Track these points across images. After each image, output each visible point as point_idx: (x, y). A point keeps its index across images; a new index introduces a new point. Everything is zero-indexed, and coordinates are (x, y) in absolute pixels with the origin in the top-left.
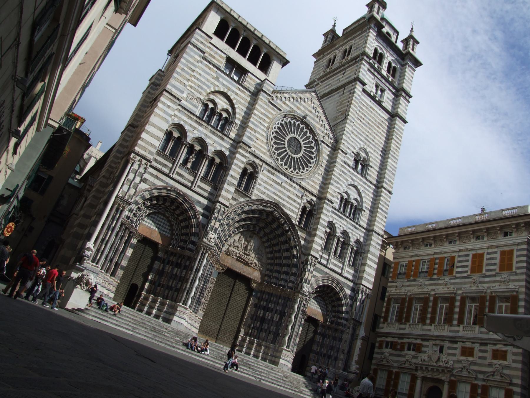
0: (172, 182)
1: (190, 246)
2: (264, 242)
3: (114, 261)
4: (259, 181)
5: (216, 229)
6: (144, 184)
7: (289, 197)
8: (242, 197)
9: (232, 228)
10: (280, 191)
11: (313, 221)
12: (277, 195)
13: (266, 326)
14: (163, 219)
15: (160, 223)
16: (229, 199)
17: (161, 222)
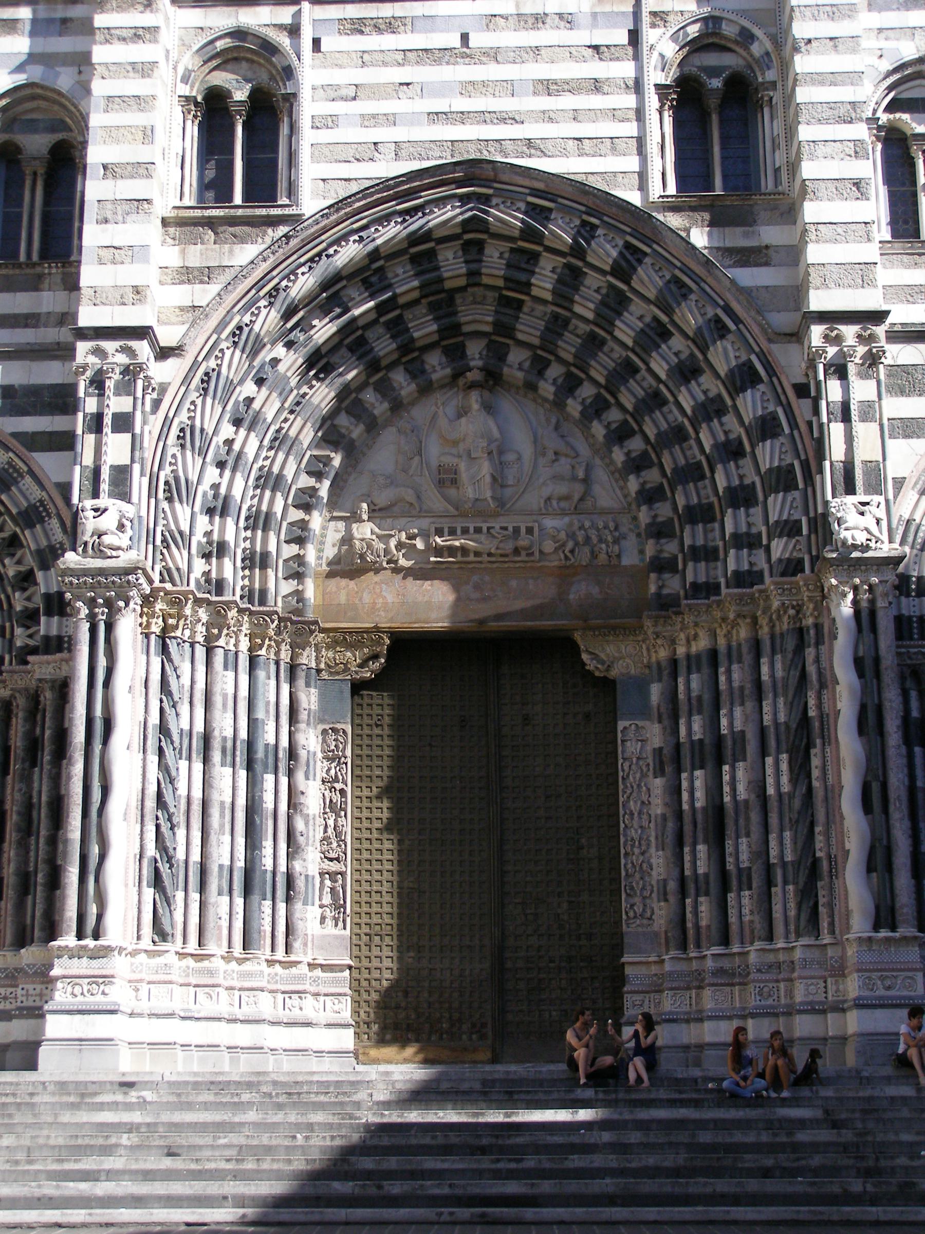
1: (48, 626)
2: (559, 404)
4: (309, 107)
5: (121, 474)
7: (548, 87)
8: (243, 241)
10: (469, 88)
11: (770, 126)
12: (463, 117)
13: (742, 851)
16: (137, 290)
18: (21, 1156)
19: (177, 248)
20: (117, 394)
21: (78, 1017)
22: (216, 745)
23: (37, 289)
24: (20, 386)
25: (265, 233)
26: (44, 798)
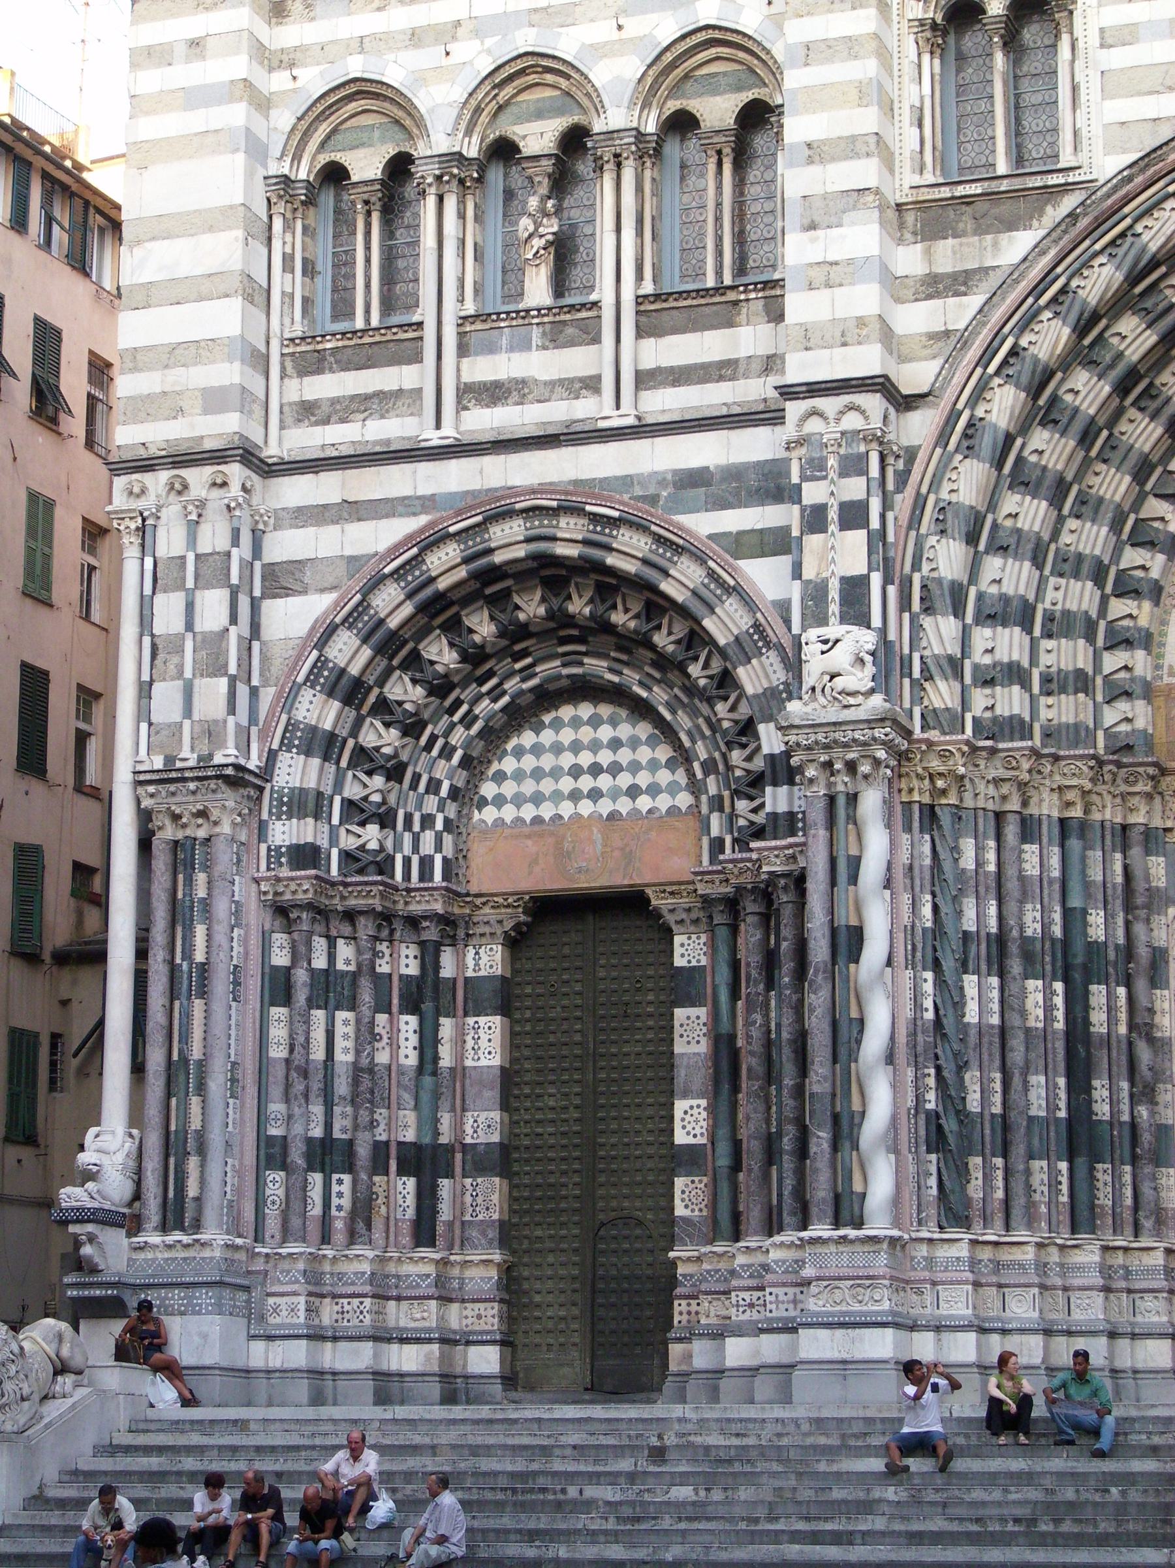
0: (456, 477)
1: (777, 799)
3: (363, 1151)
6: (293, 602)
8: (1011, 225)
9: (1112, 484)
14: (595, 722)
15: (585, 759)
16: (861, 322)
17: (595, 746)
18: (761, 1512)
19: (919, 246)
20: (844, 473)
21: (840, 1332)
22: (1014, 948)
23: (731, 324)
24: (717, 467)
25: (1041, 212)
26: (785, 1035)
